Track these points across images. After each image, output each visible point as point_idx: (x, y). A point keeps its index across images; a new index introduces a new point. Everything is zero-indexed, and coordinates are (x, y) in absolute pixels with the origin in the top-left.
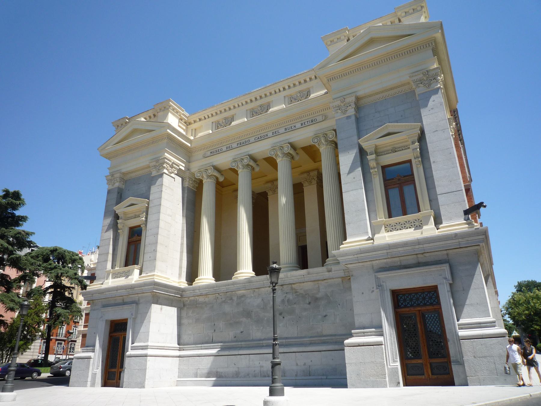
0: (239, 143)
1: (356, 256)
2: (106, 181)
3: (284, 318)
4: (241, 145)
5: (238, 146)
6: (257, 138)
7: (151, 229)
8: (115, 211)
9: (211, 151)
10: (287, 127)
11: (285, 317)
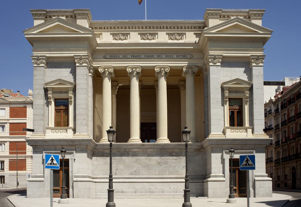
1: (217, 142)
3: (161, 166)
4: (134, 58)
6: (146, 56)
9: (111, 55)
10: (167, 55)
11: (162, 166)
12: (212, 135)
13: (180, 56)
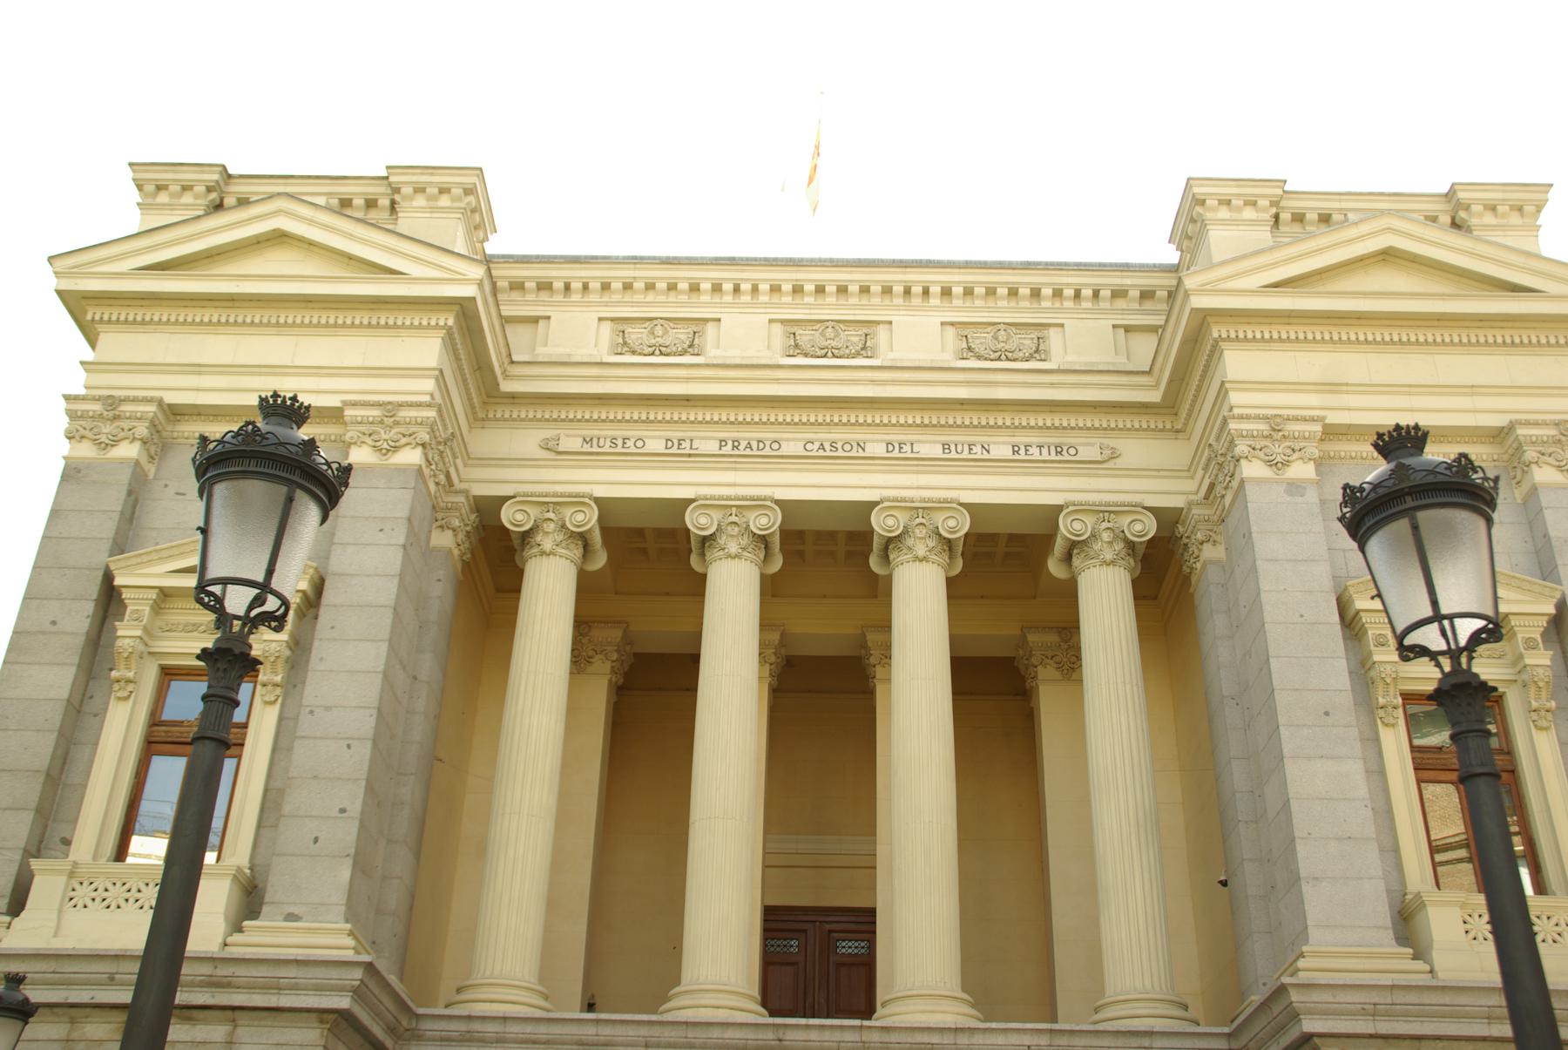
0: (730, 443)
2: (64, 421)
4: (736, 452)
5: (721, 452)
6: (817, 445)
7: (328, 708)
8: (108, 577)
12: (1316, 954)
13: (1034, 451)
